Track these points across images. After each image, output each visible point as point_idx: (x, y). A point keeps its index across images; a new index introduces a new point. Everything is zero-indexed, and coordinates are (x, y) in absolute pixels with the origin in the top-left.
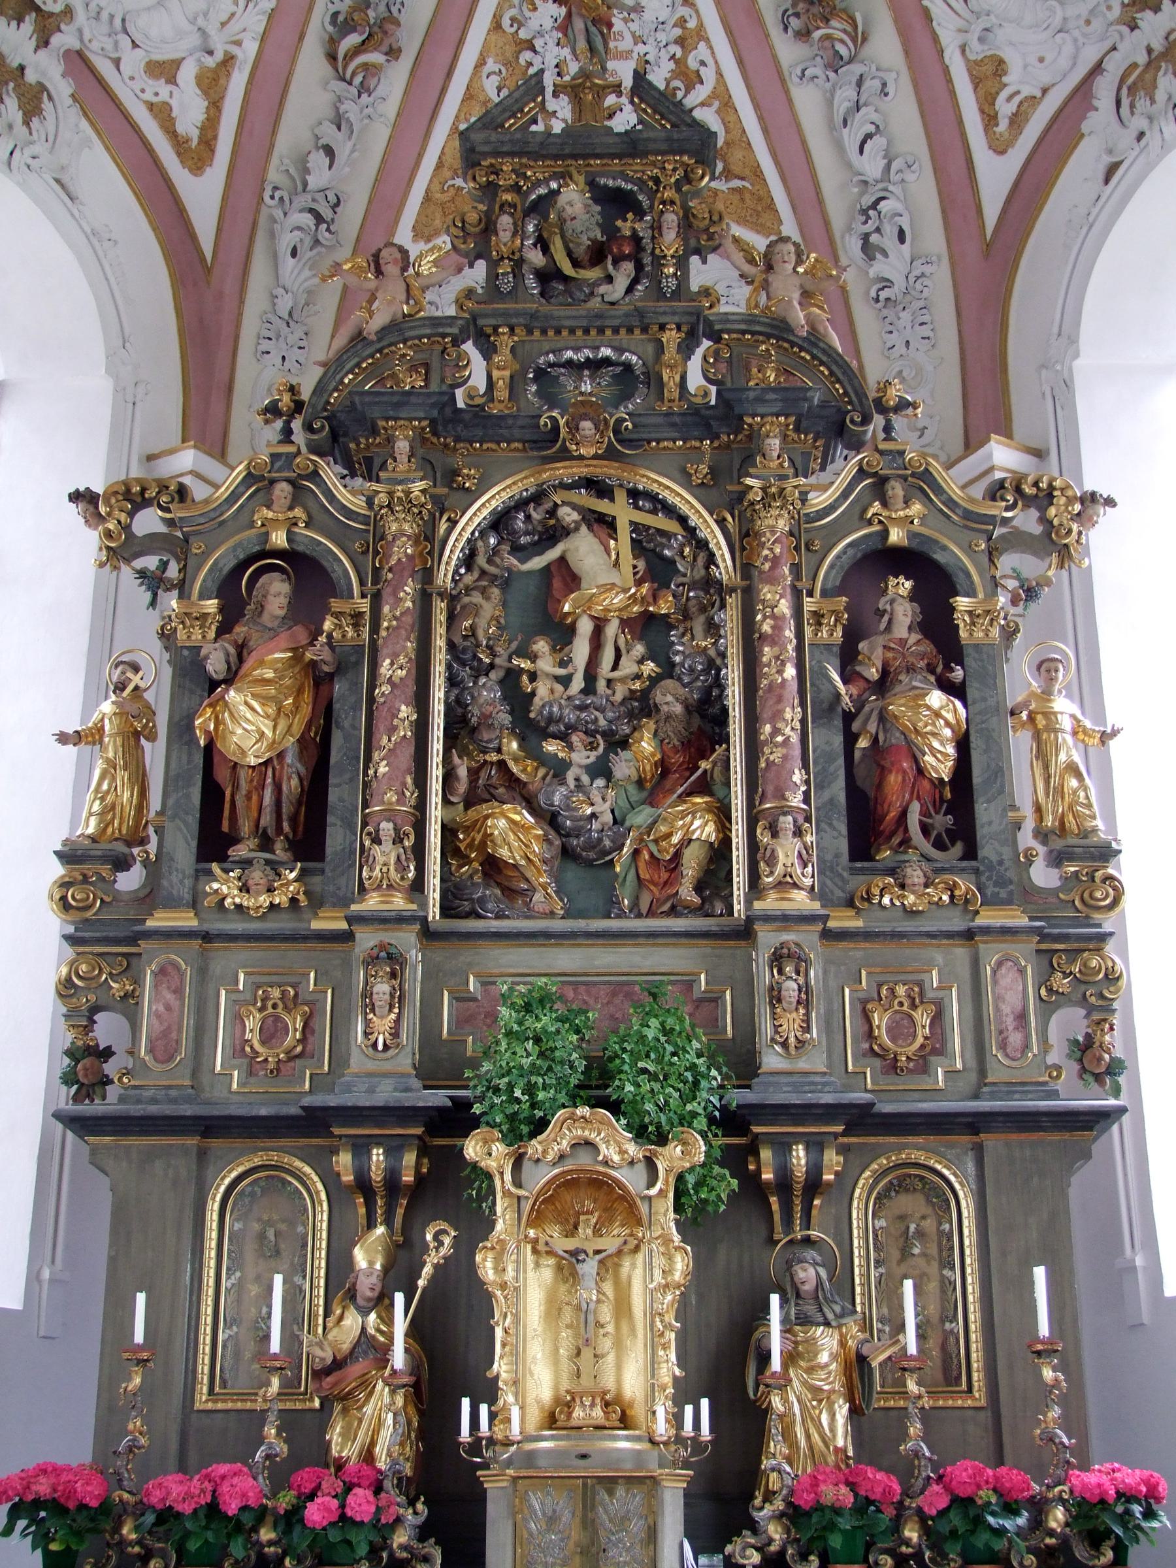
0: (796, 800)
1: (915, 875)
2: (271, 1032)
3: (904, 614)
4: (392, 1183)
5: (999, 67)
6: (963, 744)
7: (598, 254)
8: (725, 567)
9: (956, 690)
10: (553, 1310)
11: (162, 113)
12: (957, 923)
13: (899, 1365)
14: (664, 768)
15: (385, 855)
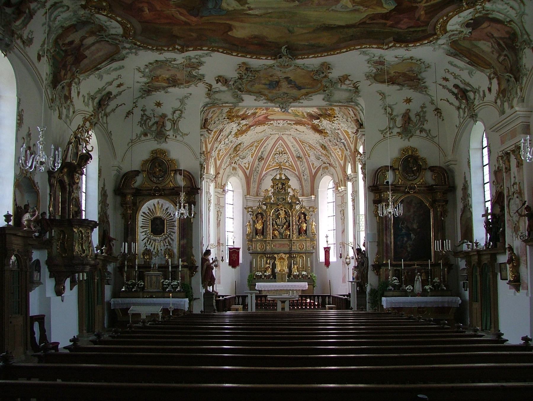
0: (295, 232)
1: (303, 236)
2: (261, 247)
3: (303, 217)
4: (270, 257)
5: (314, 164)
6: (306, 227)
7: (281, 189)
8: (291, 215)
9: (306, 223)
10: (280, 265)
11: (245, 166)
12: (305, 239)
13: (300, 268)
14: (286, 228)
15: (268, 236)
